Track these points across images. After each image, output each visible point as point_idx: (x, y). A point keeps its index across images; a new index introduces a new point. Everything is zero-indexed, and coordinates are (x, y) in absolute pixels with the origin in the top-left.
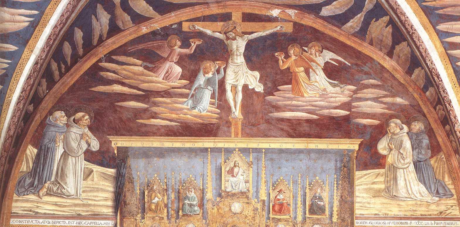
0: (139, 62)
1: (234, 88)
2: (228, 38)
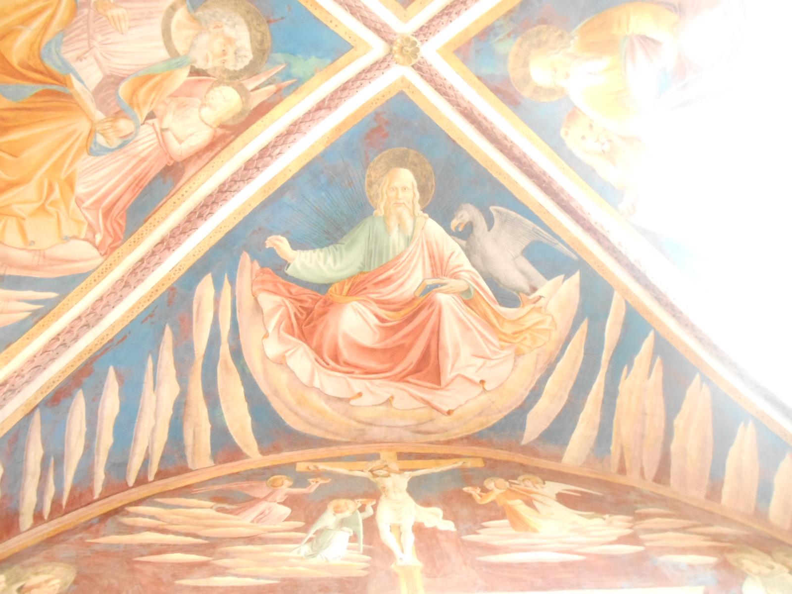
0: (209, 504)
1: (397, 529)
2: (376, 476)
